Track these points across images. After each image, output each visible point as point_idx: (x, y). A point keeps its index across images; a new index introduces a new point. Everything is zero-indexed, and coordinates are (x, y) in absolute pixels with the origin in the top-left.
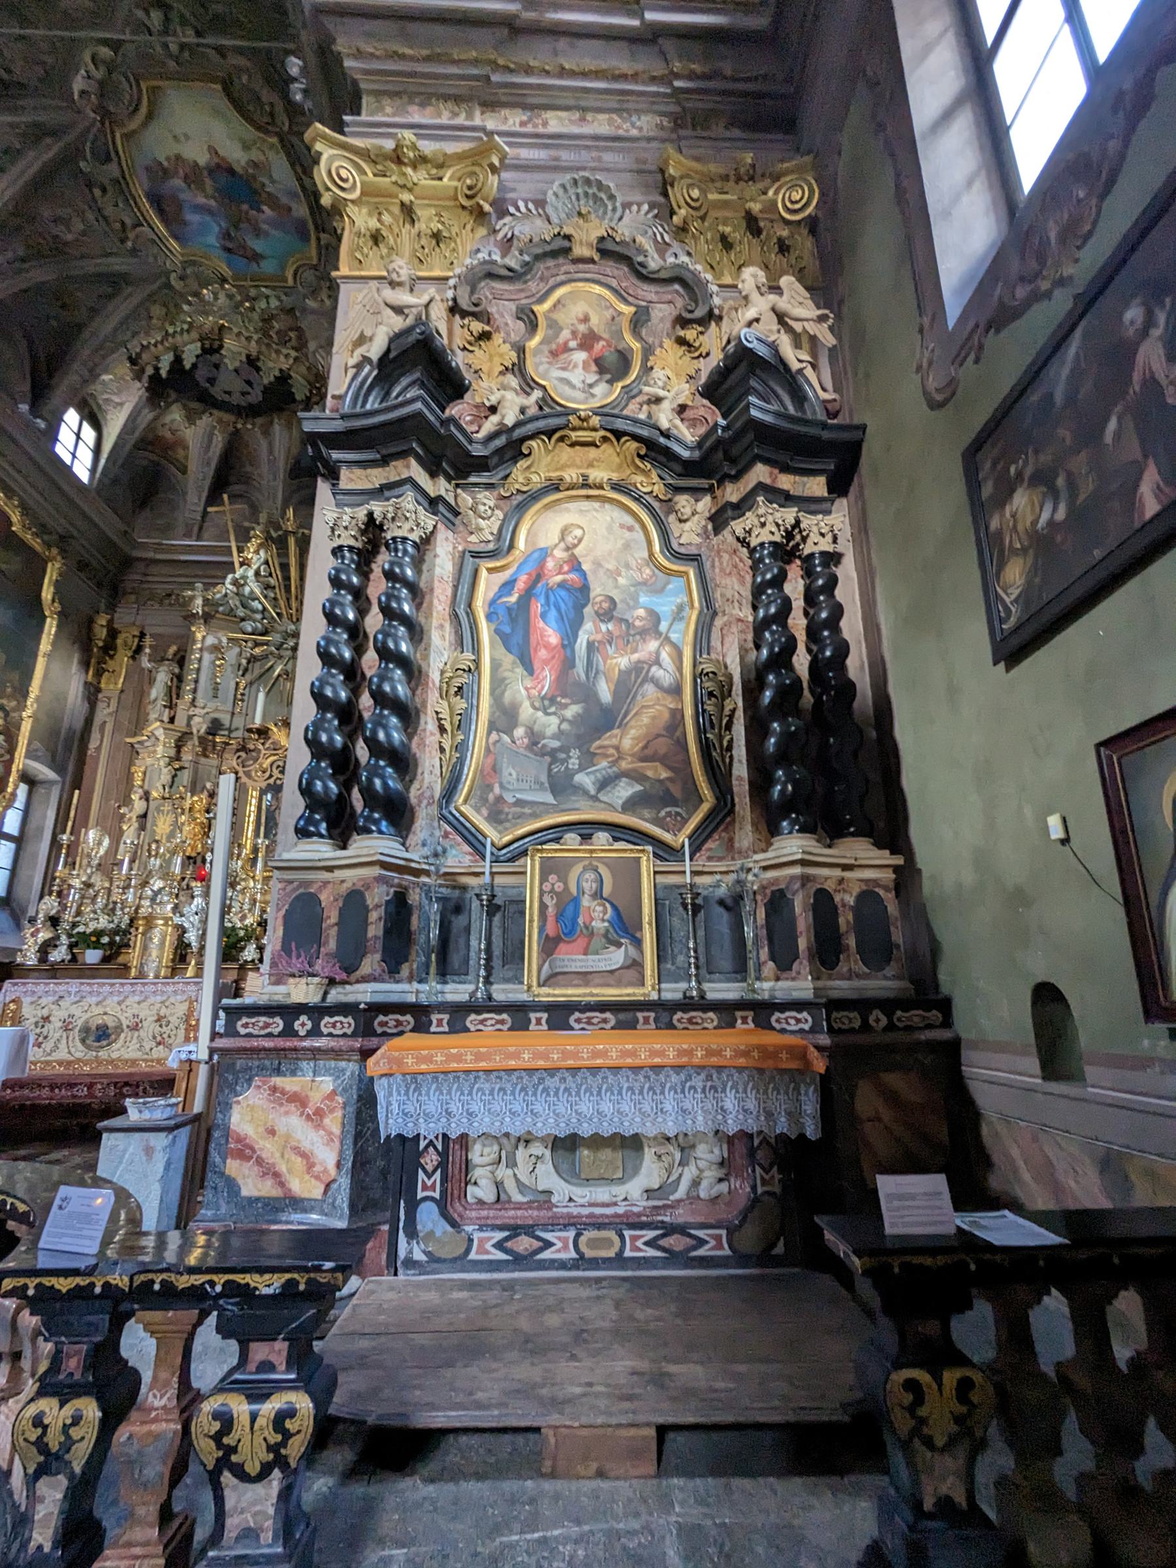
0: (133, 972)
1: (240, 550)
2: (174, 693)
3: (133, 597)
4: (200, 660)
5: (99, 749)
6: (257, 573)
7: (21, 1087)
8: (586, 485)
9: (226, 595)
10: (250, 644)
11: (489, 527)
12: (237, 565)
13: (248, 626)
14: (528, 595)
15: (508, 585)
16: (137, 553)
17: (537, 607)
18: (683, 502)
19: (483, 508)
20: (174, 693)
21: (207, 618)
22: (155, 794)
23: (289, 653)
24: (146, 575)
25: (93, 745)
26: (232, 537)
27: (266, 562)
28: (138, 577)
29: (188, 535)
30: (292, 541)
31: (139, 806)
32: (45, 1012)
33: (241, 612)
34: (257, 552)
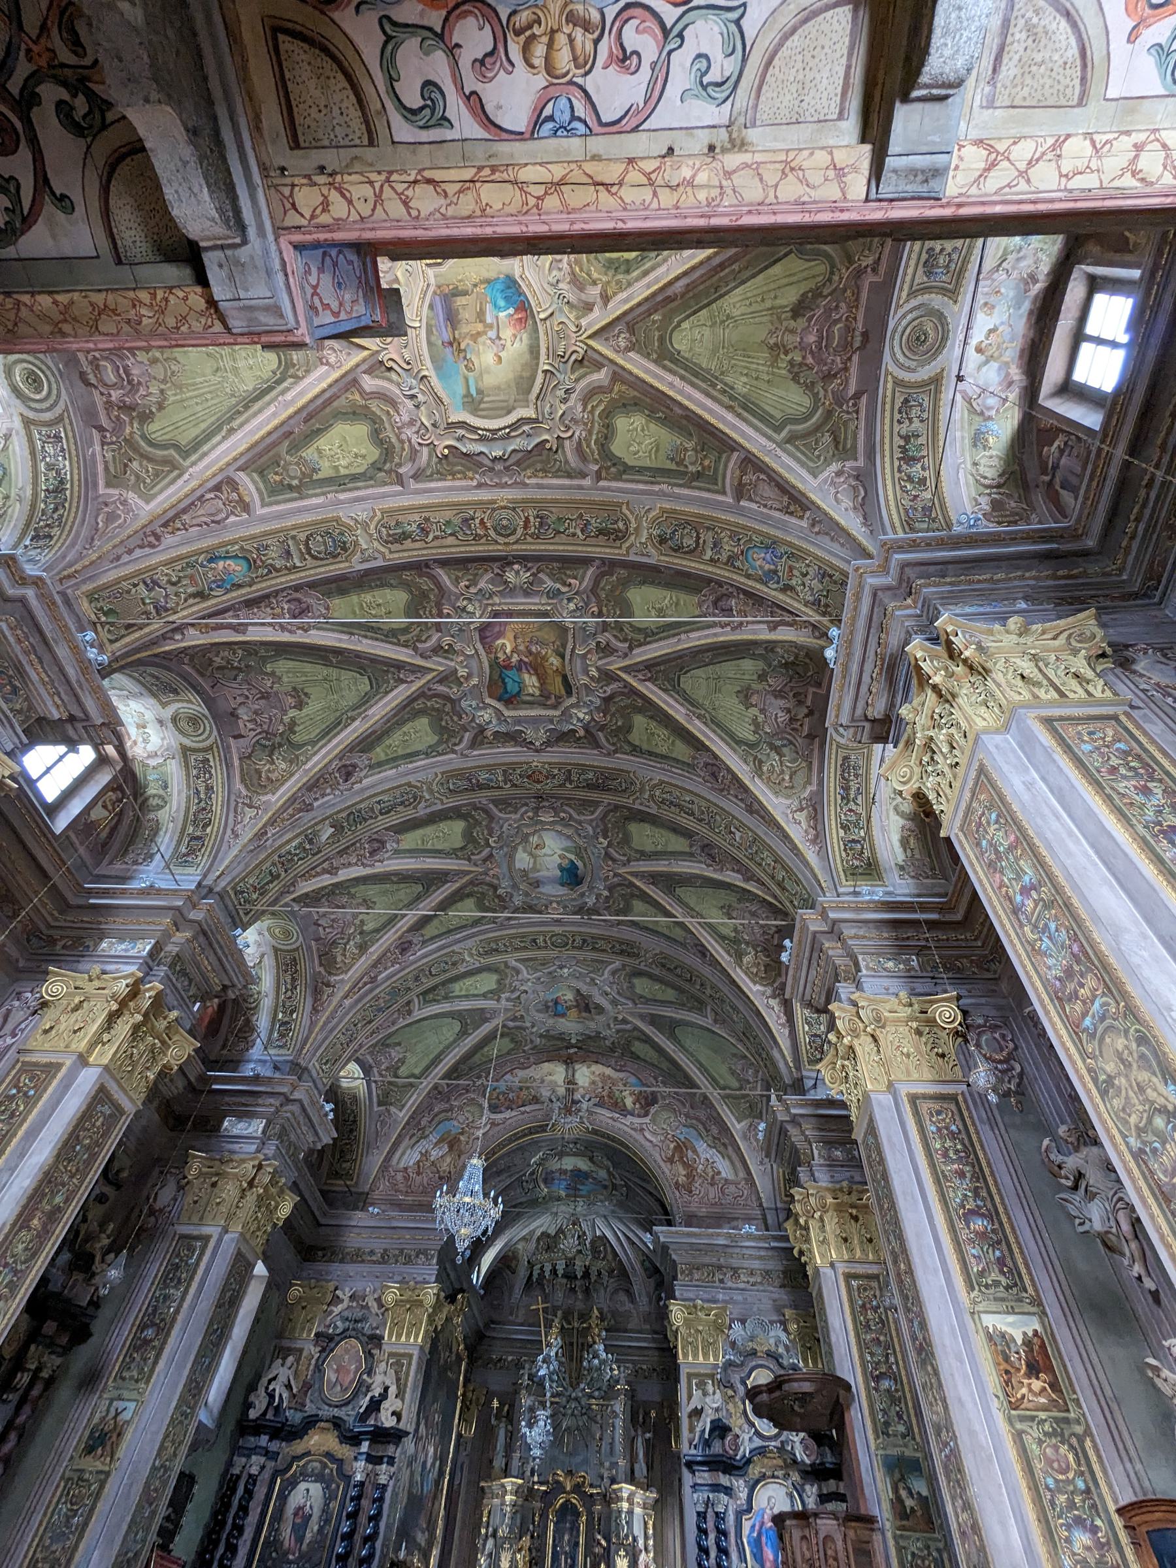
8: (773, 1477)
11: (743, 1495)
14: (760, 1534)
15: (753, 1527)
17: (764, 1539)
18: (808, 1487)
19: (740, 1485)
22: (500, 1533)
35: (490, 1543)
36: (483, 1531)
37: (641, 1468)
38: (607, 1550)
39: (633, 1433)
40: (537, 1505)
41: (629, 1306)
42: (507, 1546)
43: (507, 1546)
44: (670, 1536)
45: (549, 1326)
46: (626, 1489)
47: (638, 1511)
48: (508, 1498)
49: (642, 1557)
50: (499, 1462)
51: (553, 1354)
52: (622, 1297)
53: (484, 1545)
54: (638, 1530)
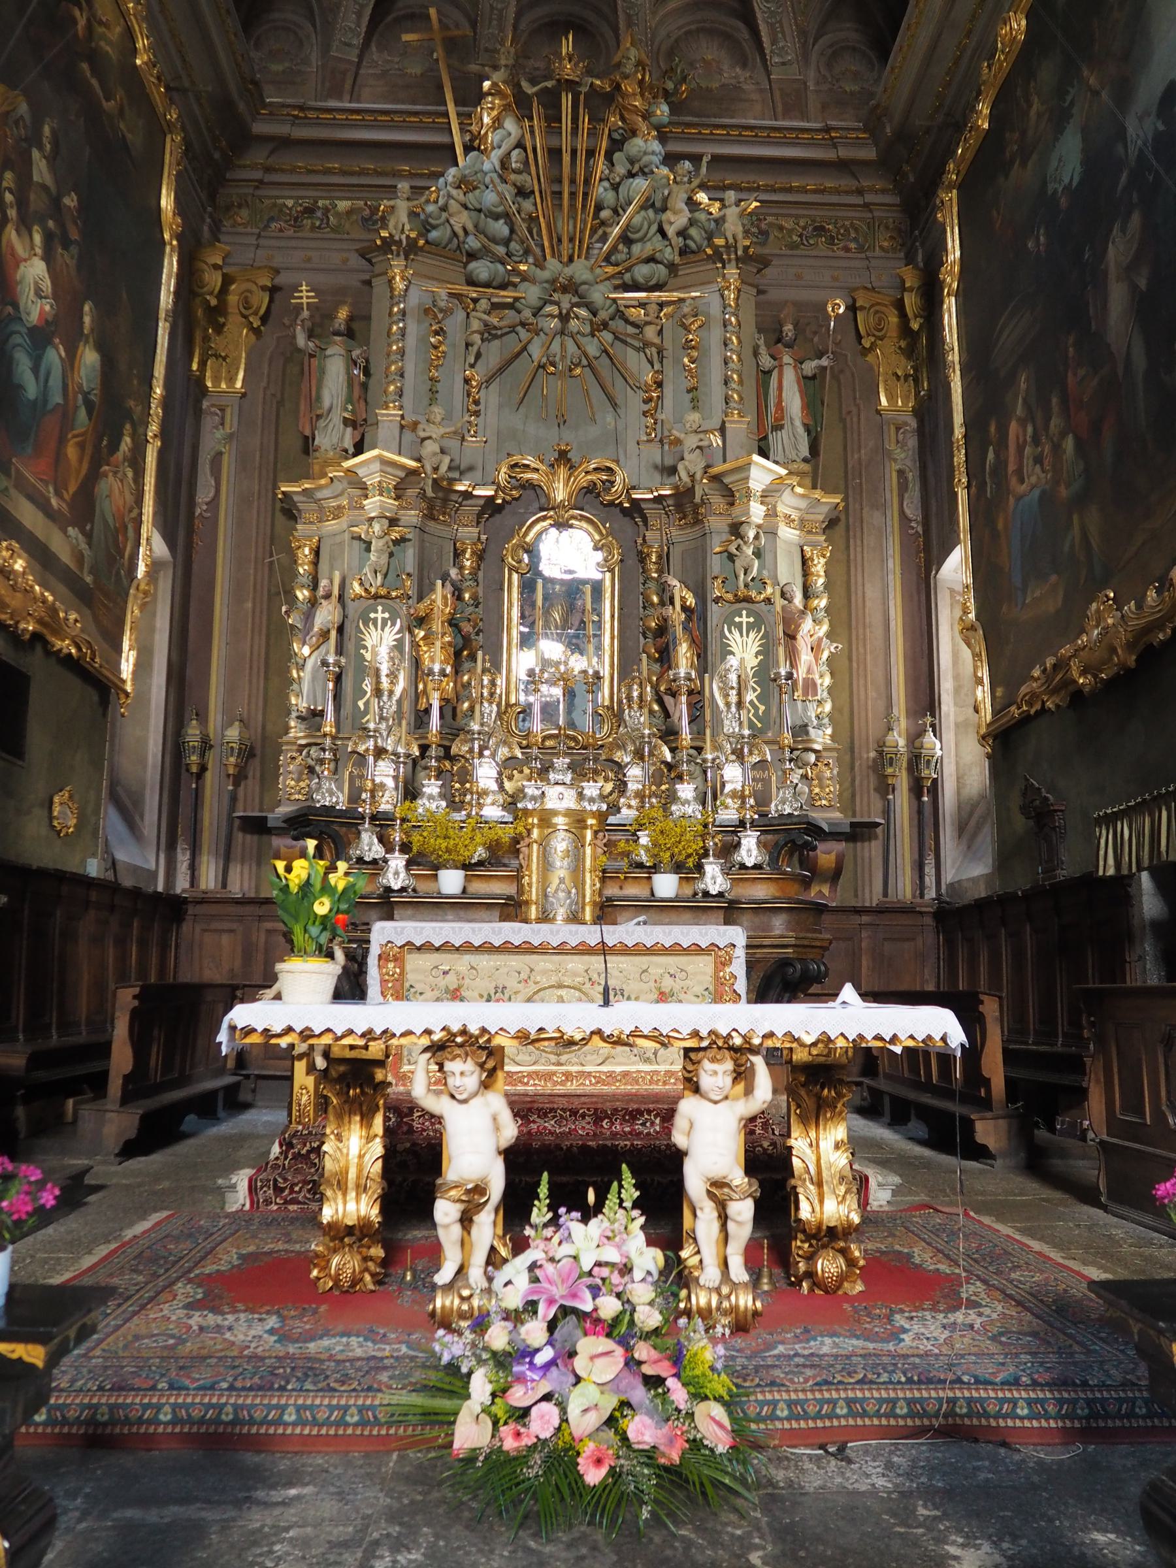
0: (533, 912)
1: (465, 118)
2: (362, 391)
3: (245, 213)
4: (403, 333)
5: (214, 503)
6: (504, 163)
7: (544, 1114)
9: (444, 209)
10: (483, 304)
12: (459, 150)
13: (482, 269)
16: (259, 128)
20: (362, 391)
21: (410, 250)
23: (554, 324)
24: (268, 170)
25: (203, 496)
26: (449, 96)
27: (520, 145)
28: (258, 175)
29: (336, 92)
30: (566, 101)
31: (326, 615)
32: (451, 981)
33: (473, 243)
34: (497, 123)
35: (326, 615)
36: (302, 594)
37: (793, 438)
38: (696, 616)
39: (766, 361)
40: (468, 533)
41: (731, 73)
42: (380, 615)
43: (380, 615)
44: (872, 593)
45: (470, 97)
46: (762, 473)
47: (788, 534)
48: (373, 504)
49: (807, 625)
50: (331, 436)
51: (491, 162)
52: (709, 51)
53: (309, 617)
54: (787, 571)
